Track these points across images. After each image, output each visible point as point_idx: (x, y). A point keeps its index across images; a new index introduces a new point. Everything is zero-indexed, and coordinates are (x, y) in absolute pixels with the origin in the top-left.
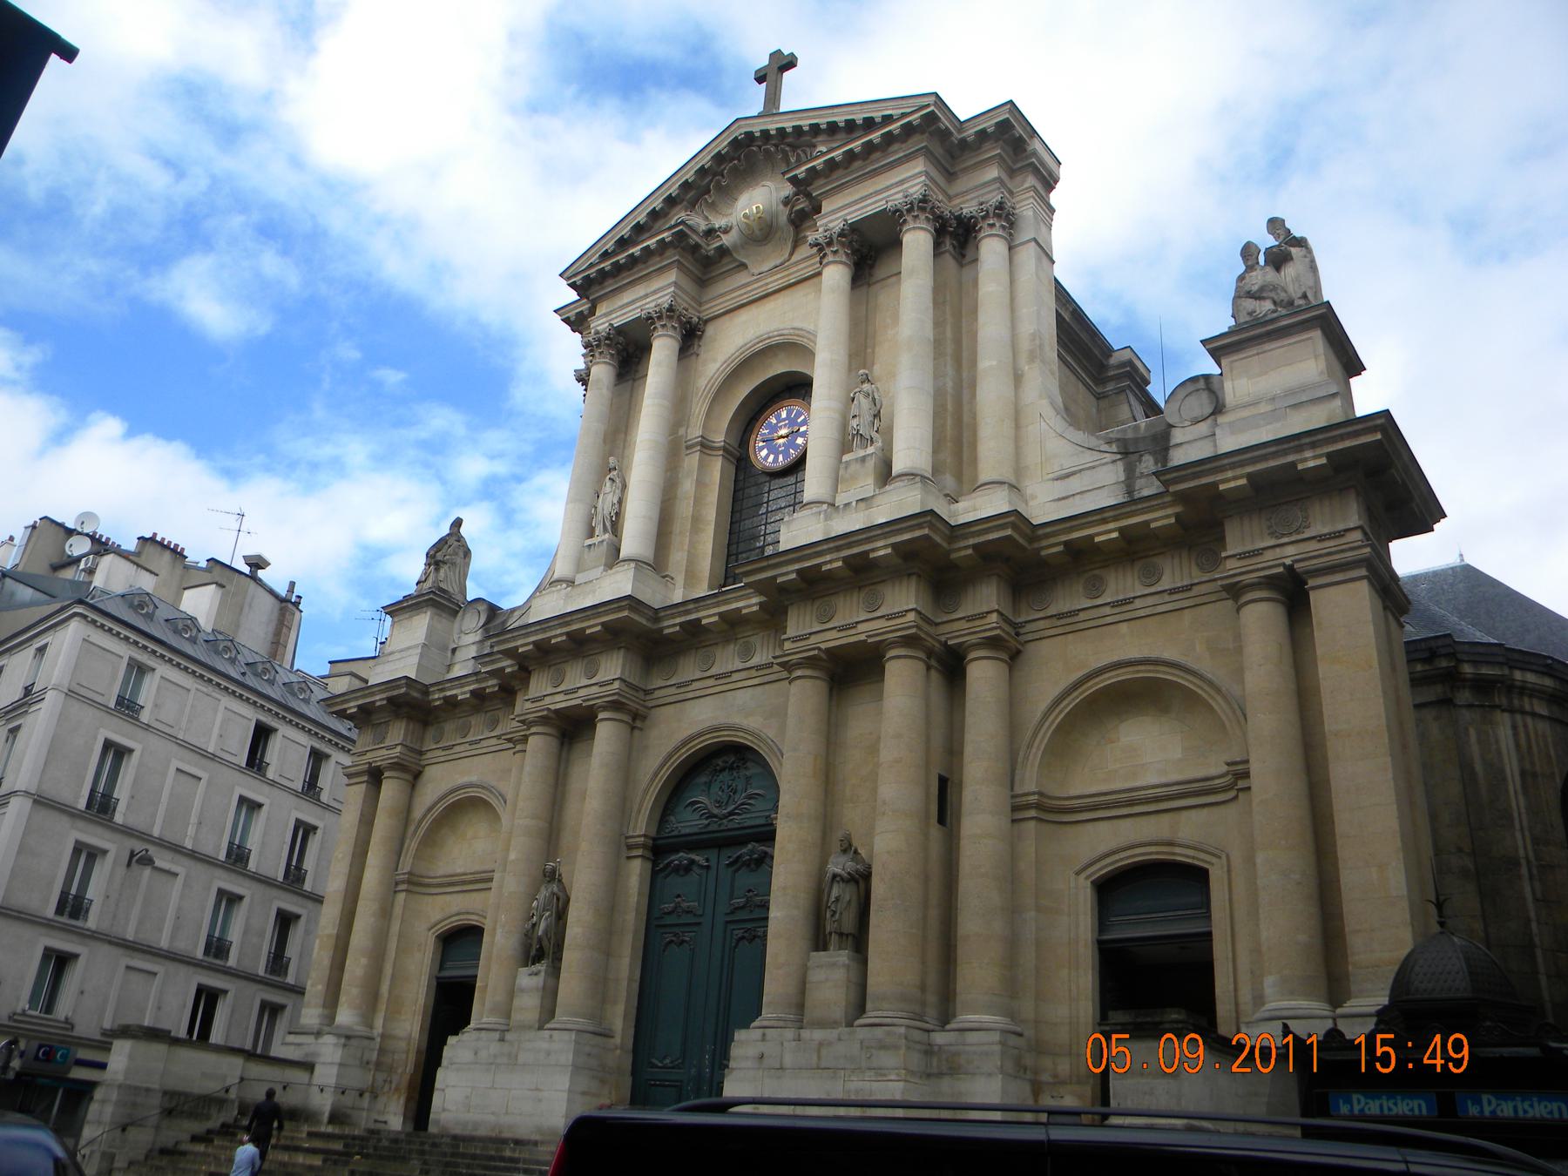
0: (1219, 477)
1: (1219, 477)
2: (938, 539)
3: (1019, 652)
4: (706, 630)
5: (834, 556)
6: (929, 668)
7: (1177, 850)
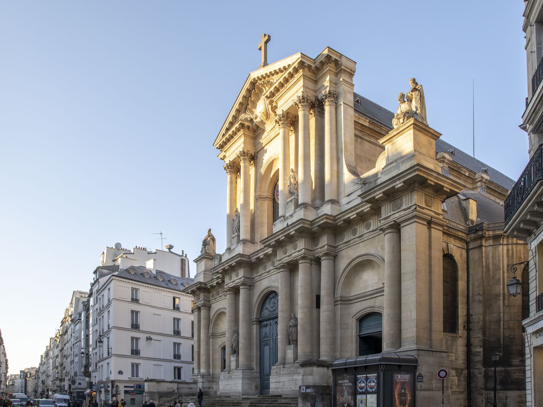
2: (307, 226)
3: (337, 255)
4: (262, 259)
6: (311, 264)
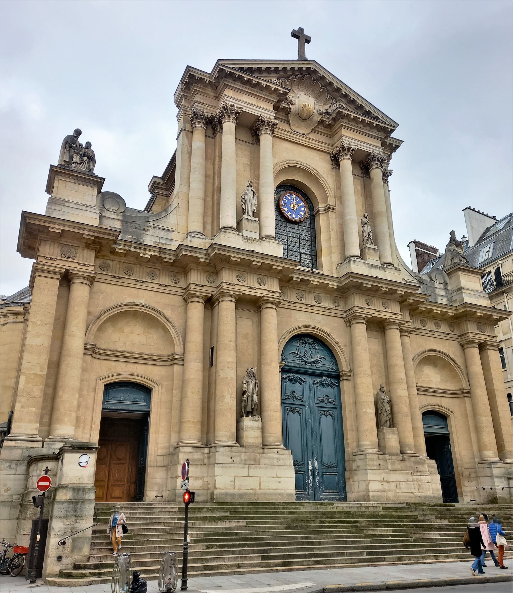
0: (478, 311)
1: (478, 311)
5: (386, 286)
7: (443, 409)
